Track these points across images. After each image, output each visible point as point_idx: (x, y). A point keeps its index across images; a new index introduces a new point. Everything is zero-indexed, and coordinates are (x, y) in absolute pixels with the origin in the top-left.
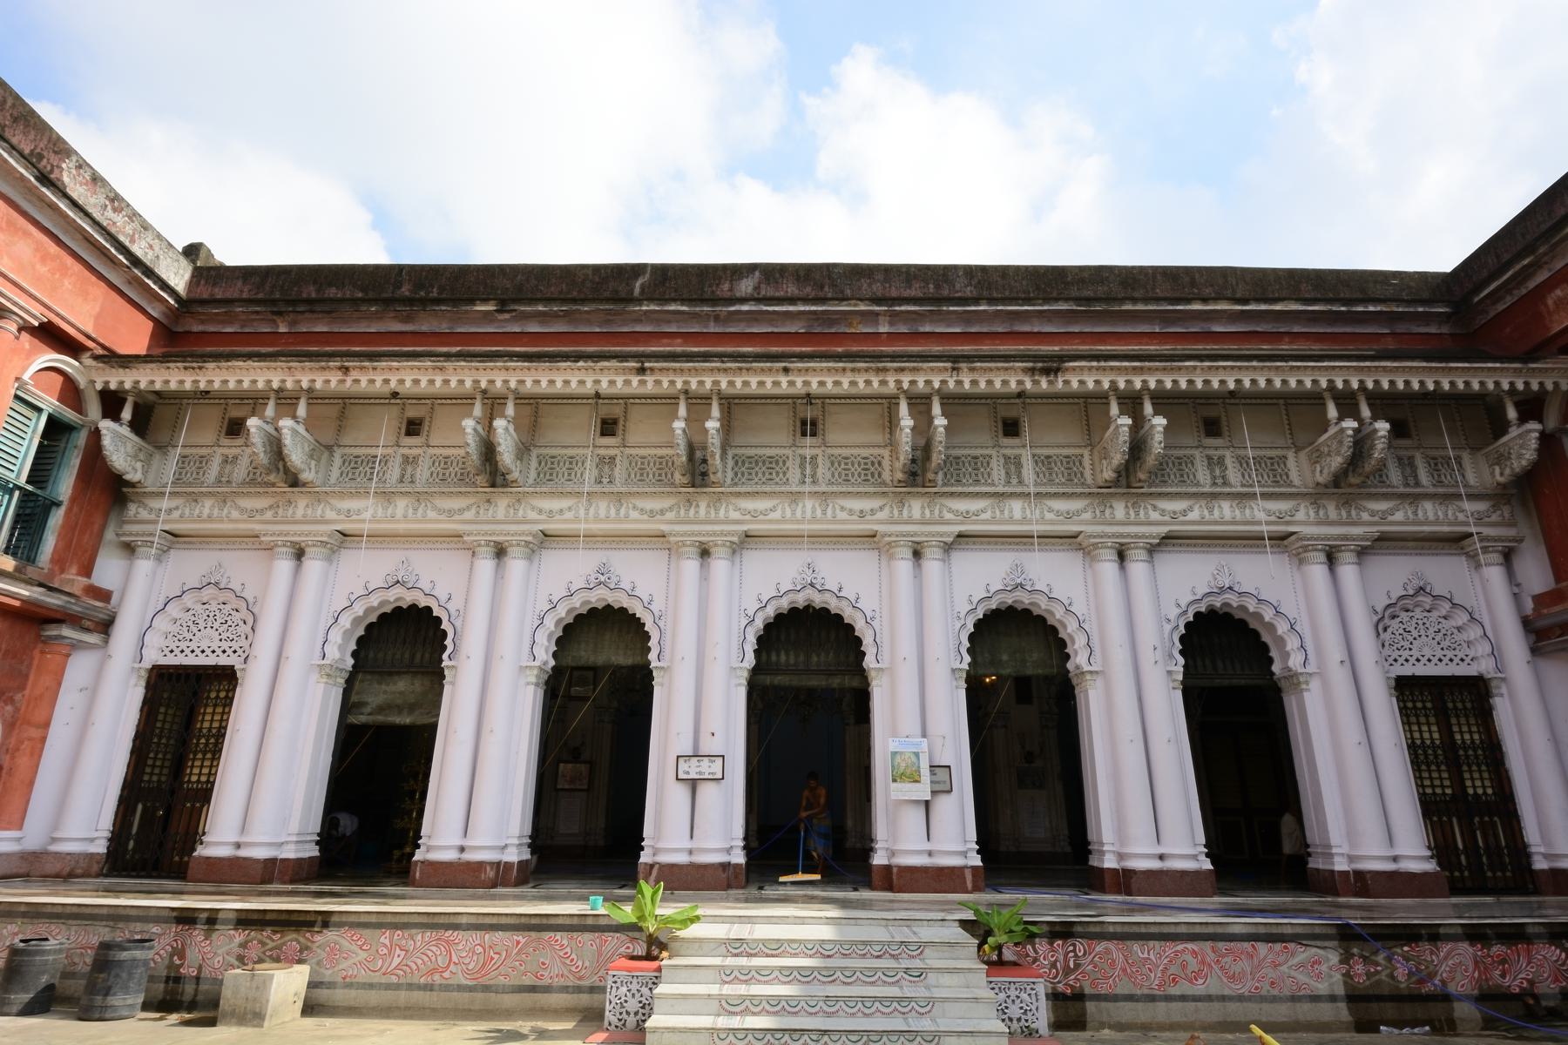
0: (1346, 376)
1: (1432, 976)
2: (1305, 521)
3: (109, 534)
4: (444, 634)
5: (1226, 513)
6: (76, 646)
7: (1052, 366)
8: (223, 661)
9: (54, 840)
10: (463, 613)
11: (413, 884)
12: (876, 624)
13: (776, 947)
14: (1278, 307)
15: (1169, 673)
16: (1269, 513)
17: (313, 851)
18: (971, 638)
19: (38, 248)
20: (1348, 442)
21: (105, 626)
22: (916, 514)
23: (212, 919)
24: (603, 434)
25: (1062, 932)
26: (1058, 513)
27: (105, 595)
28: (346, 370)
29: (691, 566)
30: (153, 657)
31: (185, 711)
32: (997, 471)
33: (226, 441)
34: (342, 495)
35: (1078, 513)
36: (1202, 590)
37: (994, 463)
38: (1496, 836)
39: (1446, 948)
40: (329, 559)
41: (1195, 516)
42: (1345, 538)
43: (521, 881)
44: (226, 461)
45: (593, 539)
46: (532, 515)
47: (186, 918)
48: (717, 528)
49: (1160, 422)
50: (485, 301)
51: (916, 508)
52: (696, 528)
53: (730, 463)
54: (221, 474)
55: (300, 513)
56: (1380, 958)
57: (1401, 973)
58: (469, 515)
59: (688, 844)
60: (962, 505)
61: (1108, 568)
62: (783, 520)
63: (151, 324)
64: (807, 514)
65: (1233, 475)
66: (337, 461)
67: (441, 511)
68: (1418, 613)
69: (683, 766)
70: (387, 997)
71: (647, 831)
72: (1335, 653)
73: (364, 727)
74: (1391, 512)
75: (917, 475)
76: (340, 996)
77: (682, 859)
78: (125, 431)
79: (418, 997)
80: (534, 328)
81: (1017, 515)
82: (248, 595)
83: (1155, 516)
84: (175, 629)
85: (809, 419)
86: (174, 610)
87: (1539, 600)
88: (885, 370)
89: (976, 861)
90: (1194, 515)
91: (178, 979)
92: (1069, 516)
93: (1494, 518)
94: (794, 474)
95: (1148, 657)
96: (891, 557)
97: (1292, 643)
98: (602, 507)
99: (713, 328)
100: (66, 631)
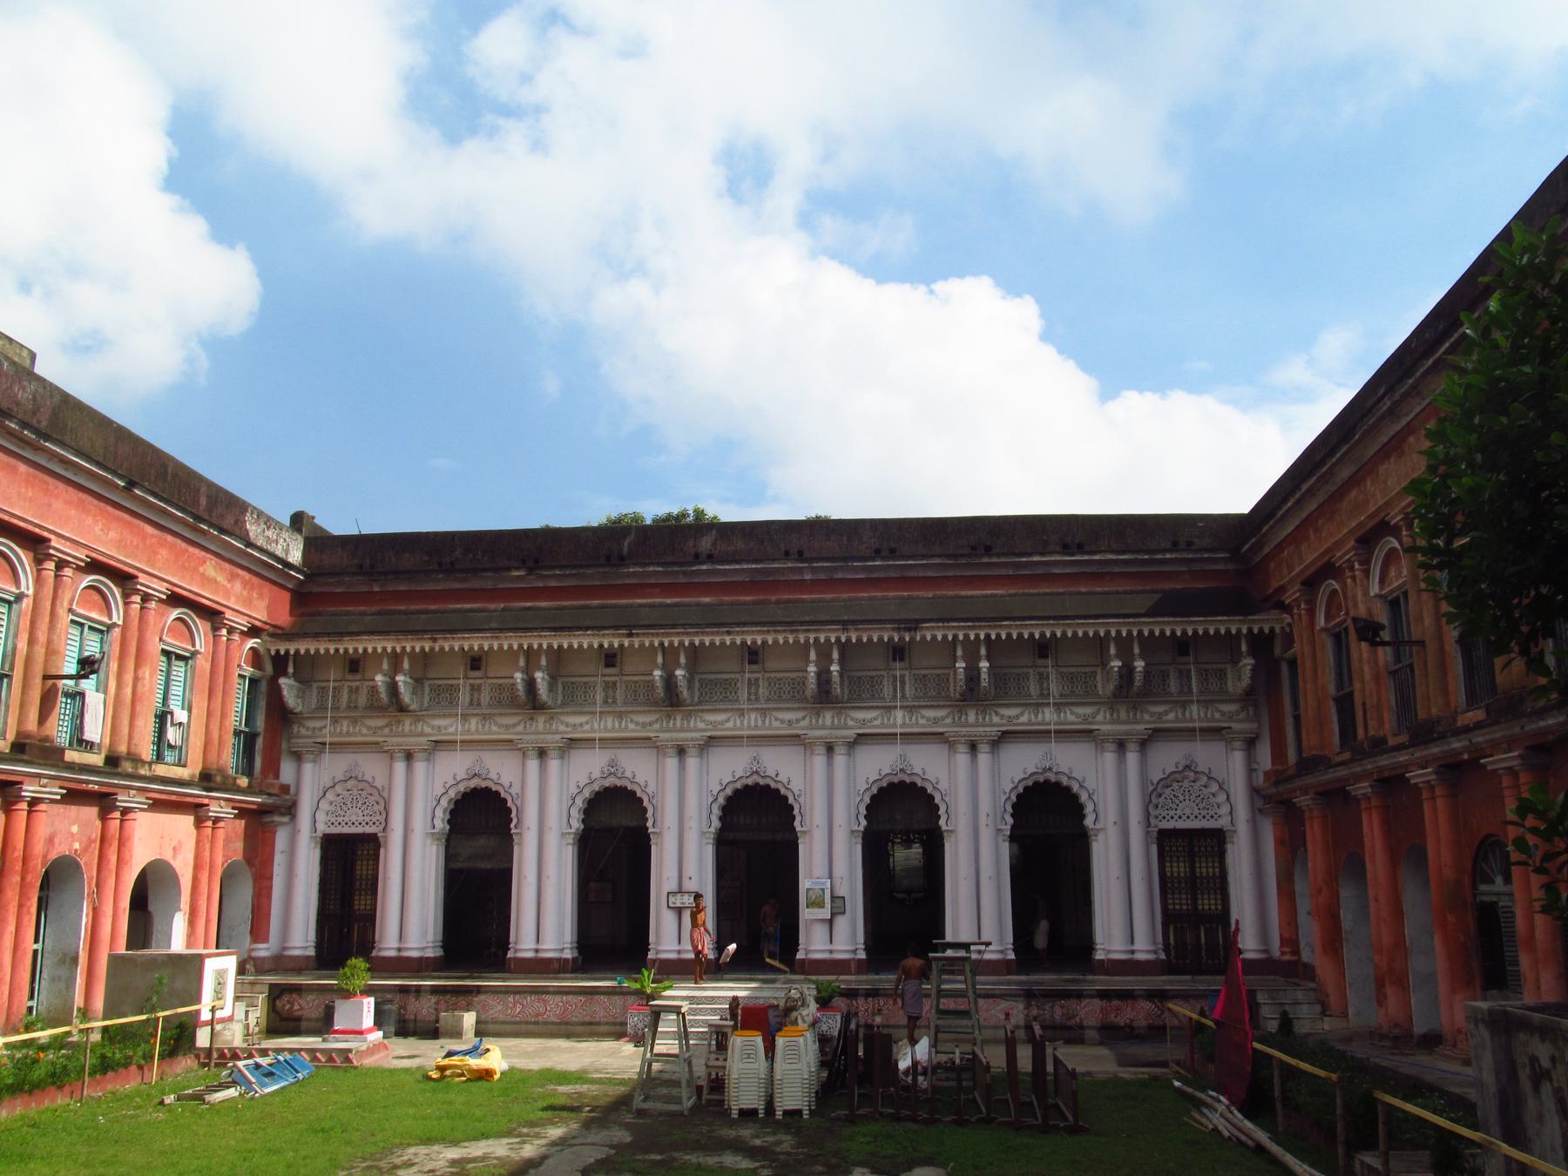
0: (1114, 627)
1: (1074, 1017)
2: (1103, 722)
3: (284, 746)
4: (510, 811)
5: (1049, 716)
6: (283, 824)
7: (913, 625)
8: (369, 830)
9: (285, 949)
10: (522, 795)
11: (509, 971)
12: (801, 800)
13: (712, 1000)
14: (1097, 557)
15: (999, 831)
16: (1078, 716)
17: (440, 953)
18: (868, 808)
19: (245, 584)
20: (1116, 676)
21: (291, 810)
22: (828, 721)
23: (418, 989)
24: (608, 665)
25: (873, 993)
26: (928, 719)
27: (285, 789)
28: (435, 640)
29: (672, 763)
30: (322, 828)
31: (350, 865)
32: (887, 690)
33: (350, 677)
34: (434, 717)
35: (943, 718)
36: (1031, 770)
37: (885, 682)
38: (1198, 937)
39: (1086, 1001)
40: (428, 760)
41: (1024, 718)
42: (1127, 733)
43: (574, 971)
44: (351, 691)
45: (606, 743)
46: (562, 728)
47: (404, 990)
48: (689, 735)
49: (984, 664)
50: (518, 569)
51: (828, 718)
52: (675, 735)
53: (697, 685)
54: (350, 701)
55: (407, 728)
56: (1047, 1007)
57: (1058, 1012)
58: (520, 728)
59: (677, 948)
60: (860, 715)
61: (962, 758)
62: (735, 728)
63: (287, 596)
64: (751, 722)
65: (1054, 687)
66: (427, 690)
67: (500, 726)
68: (1186, 783)
69: (672, 899)
70: (516, 1028)
71: (652, 938)
72: (1110, 814)
73: (461, 871)
74: (1166, 713)
75: (824, 697)
76: (491, 1027)
77: (673, 956)
78: (291, 682)
79: (531, 1027)
80: (553, 583)
81: (899, 721)
82: (378, 784)
83: (996, 719)
84: (332, 808)
85: (753, 655)
86: (330, 796)
87: (1266, 774)
88: (797, 631)
89: (862, 955)
90: (1024, 719)
91: (405, 1021)
92: (936, 721)
93: (1242, 716)
94: (743, 694)
95: (983, 820)
96: (812, 753)
97: (1089, 809)
98: (609, 721)
99: (682, 580)
100: (276, 818)
